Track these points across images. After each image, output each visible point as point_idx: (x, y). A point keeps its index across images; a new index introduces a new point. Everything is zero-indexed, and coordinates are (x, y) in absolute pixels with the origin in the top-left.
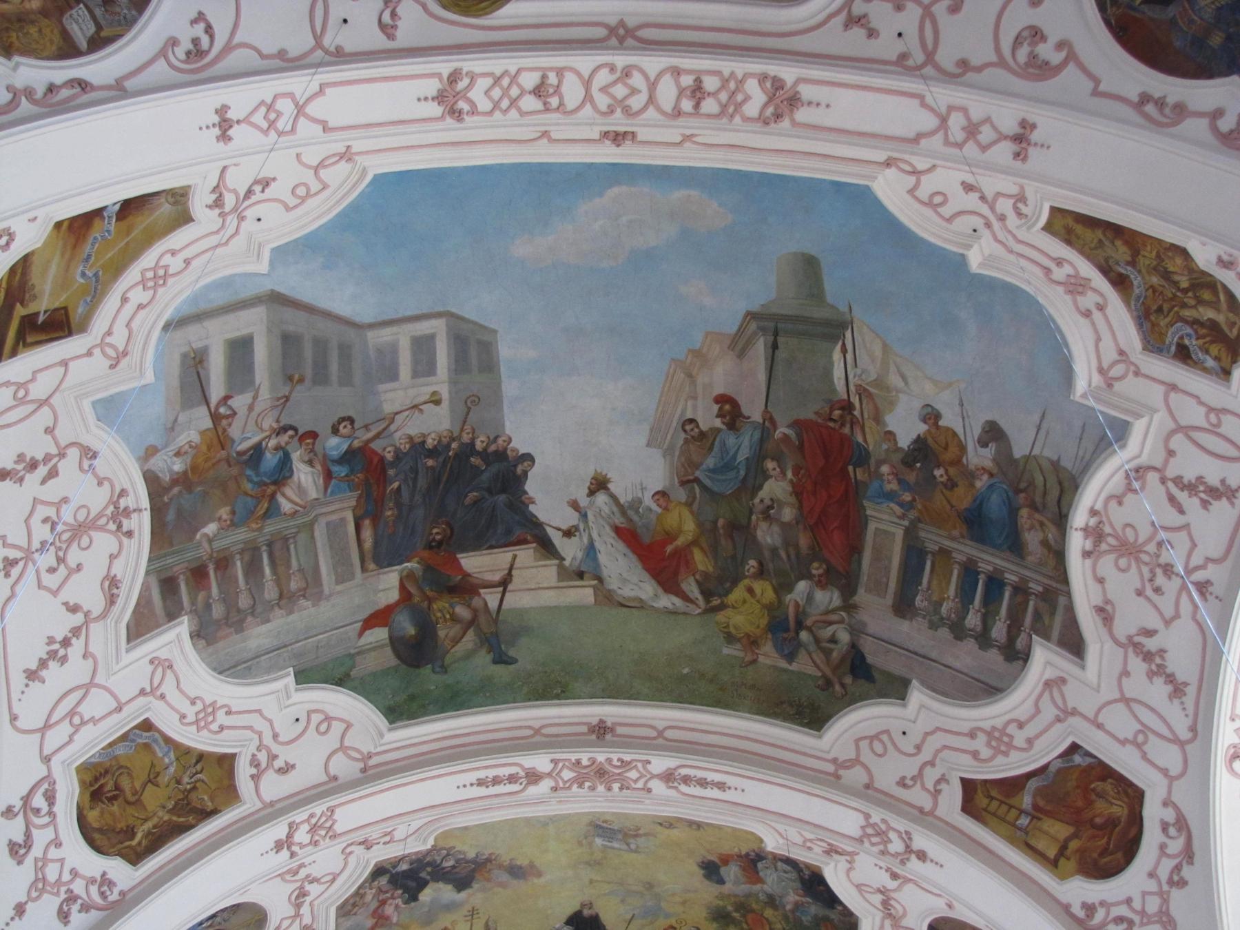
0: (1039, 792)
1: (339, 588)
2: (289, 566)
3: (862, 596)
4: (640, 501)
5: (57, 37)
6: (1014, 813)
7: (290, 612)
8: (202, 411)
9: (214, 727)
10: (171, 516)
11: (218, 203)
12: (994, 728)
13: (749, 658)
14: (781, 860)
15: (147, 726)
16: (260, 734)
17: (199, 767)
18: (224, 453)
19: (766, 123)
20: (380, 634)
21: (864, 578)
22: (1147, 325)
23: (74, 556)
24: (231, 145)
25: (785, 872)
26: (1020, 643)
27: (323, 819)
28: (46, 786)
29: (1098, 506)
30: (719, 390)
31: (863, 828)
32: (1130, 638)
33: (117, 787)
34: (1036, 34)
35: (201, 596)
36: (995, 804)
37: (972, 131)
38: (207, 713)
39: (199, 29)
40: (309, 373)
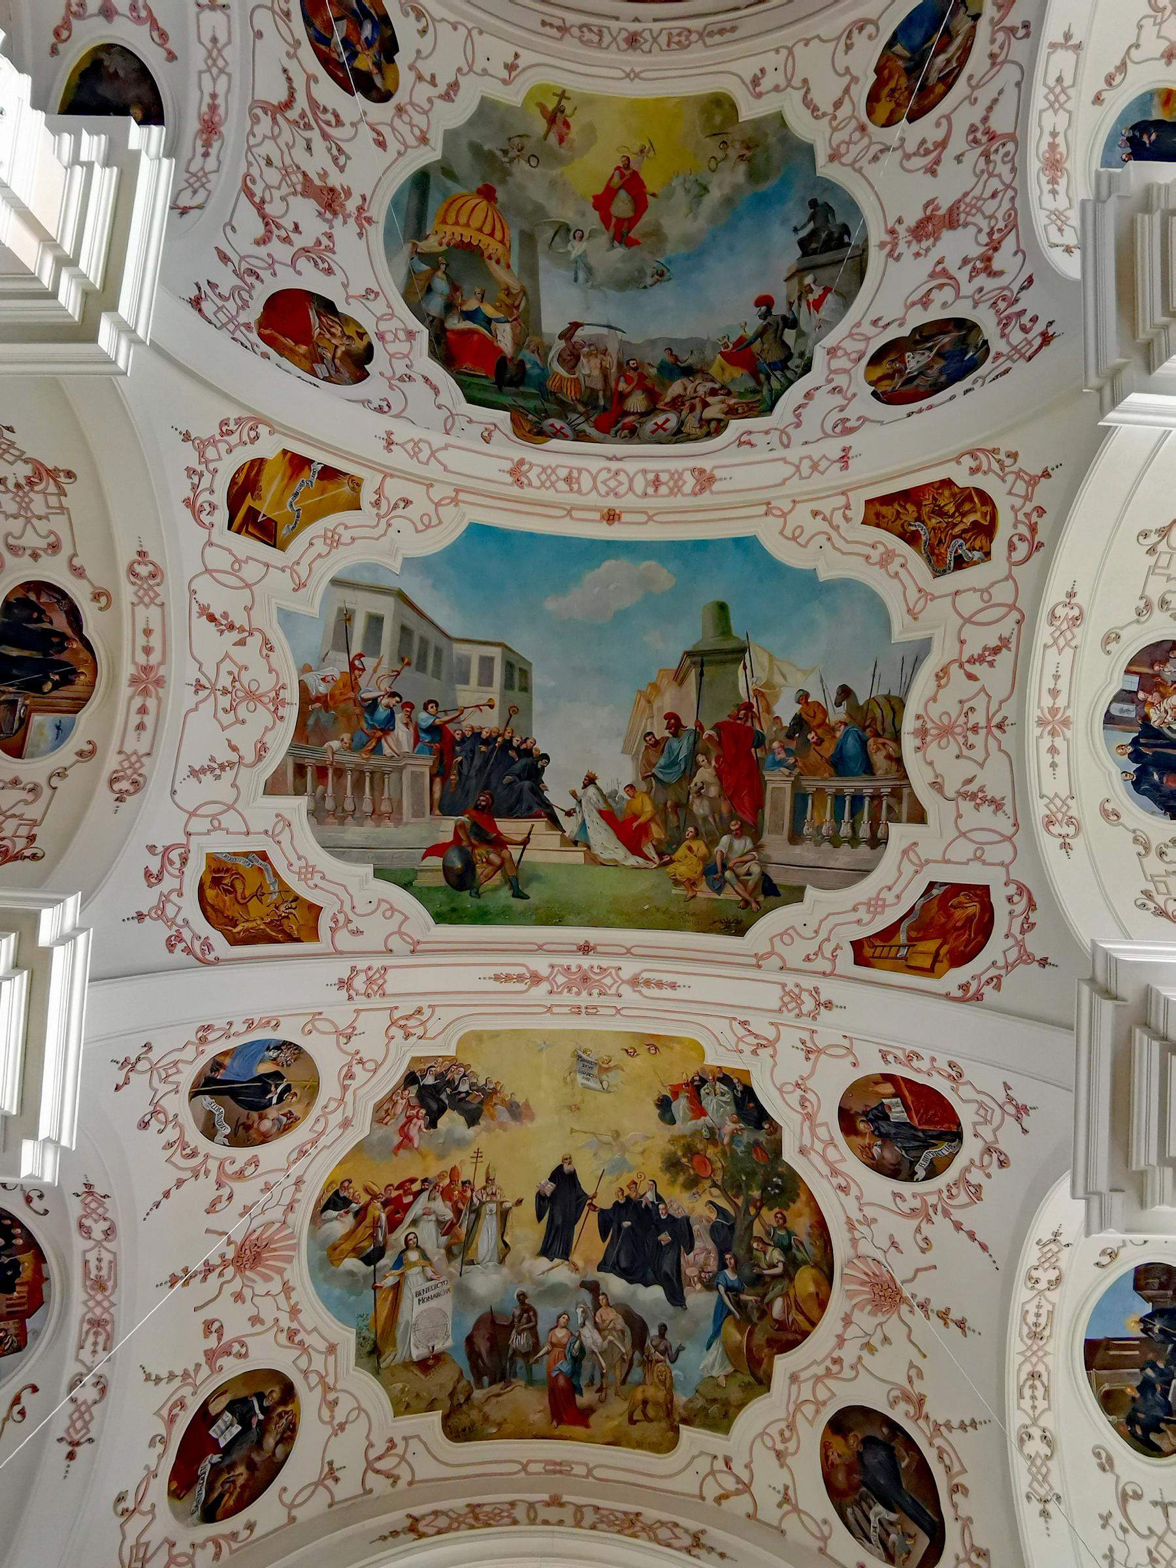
0: (910, 928)
1: (413, 820)
2: (382, 794)
3: (766, 838)
4: (616, 792)
6: (894, 950)
7: (378, 826)
9: (311, 883)
10: (311, 722)
11: (377, 504)
12: (870, 900)
13: (691, 894)
14: (720, 1080)
15: (264, 856)
16: (342, 902)
17: (294, 905)
18: (352, 695)
20: (436, 862)
21: (767, 824)
23: (242, 711)
25: (723, 1095)
26: (879, 835)
27: (377, 975)
28: (183, 850)
29: (921, 712)
31: (782, 999)
32: (958, 792)
33: (232, 886)
35: (320, 788)
36: (879, 950)
37: (815, 467)
38: (308, 871)
39: (384, 404)
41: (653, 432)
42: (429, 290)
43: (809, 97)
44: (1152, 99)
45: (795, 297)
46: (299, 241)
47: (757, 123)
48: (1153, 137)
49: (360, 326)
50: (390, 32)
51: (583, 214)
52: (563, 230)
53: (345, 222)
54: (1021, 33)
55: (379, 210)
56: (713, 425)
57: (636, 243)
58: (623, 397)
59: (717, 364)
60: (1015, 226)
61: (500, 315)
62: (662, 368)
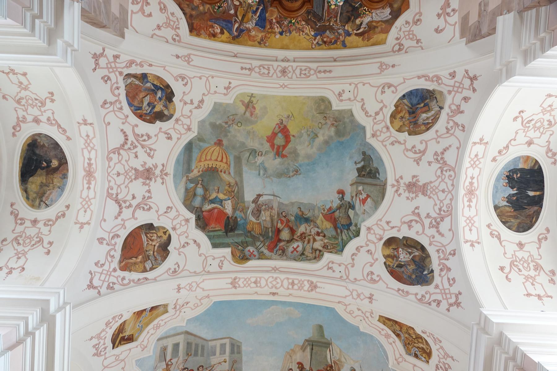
5: (142, 268)
8: (164, 362)
11: (175, 308)
19: (309, 291)
22: (406, 348)
24: (180, 293)
30: (298, 361)
34: (372, 273)
37: (359, 295)
40: (193, 353)
41: (292, 252)
42: (195, 195)
43: (364, 107)
44: (519, 160)
45: (354, 194)
46: (134, 203)
47: (340, 112)
48: (519, 175)
49: (164, 228)
50: (170, 90)
51: (262, 144)
52: (254, 152)
53: (155, 181)
54: (460, 128)
55: (170, 169)
56: (318, 252)
57: (286, 156)
58: (279, 231)
59: (320, 219)
60: (451, 214)
61: (226, 197)
62: (297, 217)
